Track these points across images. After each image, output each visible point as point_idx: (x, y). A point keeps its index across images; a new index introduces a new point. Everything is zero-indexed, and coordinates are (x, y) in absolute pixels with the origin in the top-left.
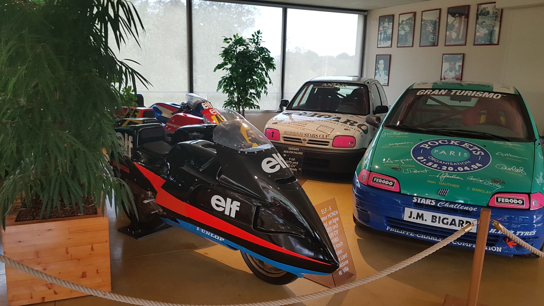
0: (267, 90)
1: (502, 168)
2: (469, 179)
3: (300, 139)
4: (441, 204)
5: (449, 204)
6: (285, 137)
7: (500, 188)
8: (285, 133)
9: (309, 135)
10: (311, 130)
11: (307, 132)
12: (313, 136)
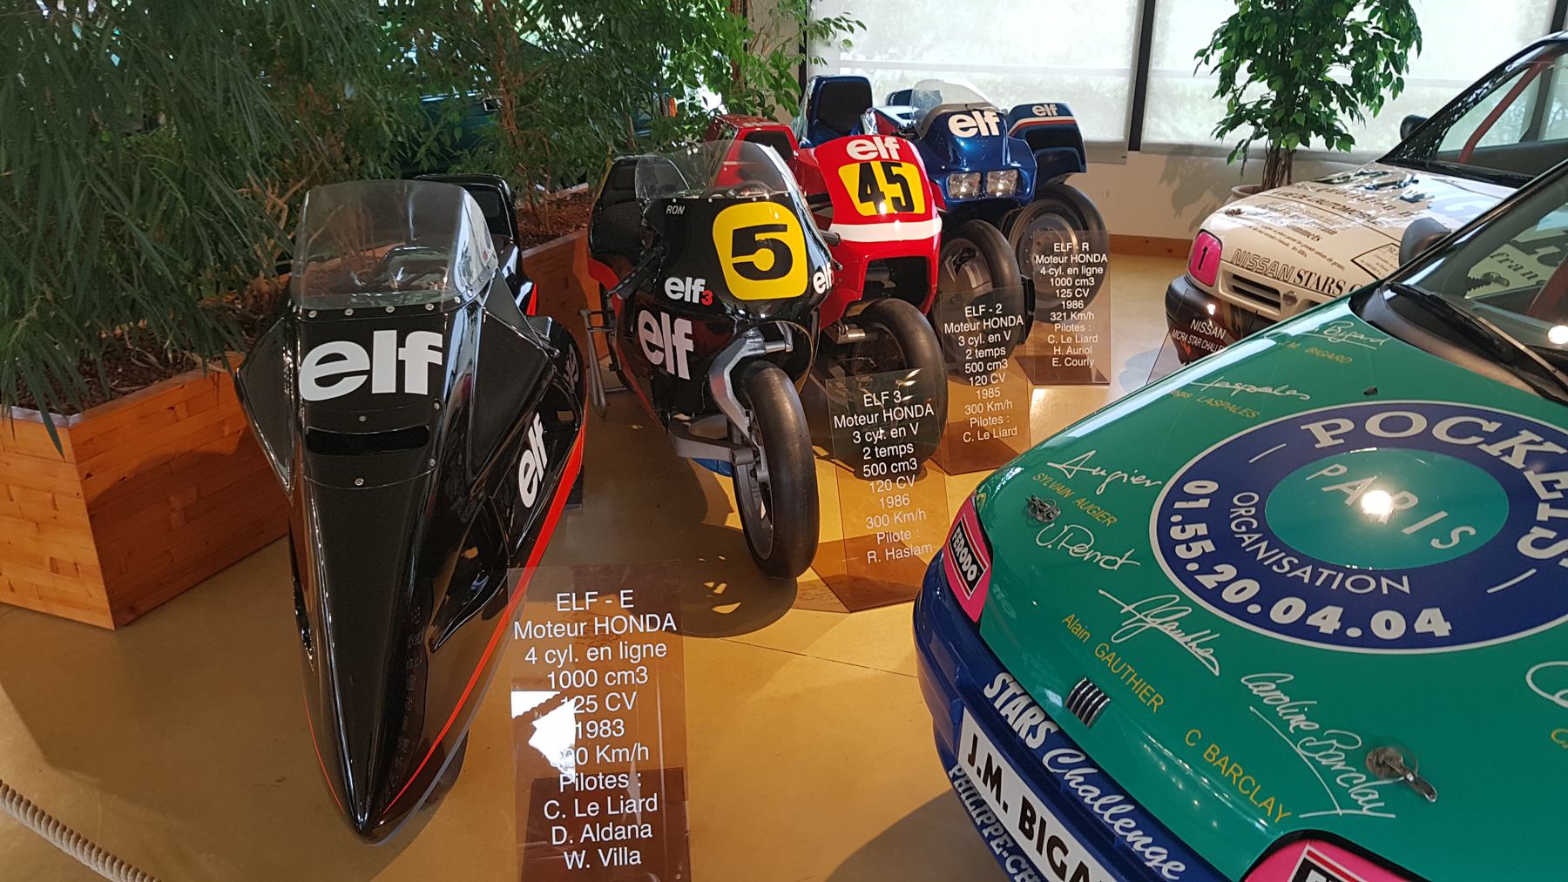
0: (1404, 71)
1: (1556, 698)
2: (1250, 686)
3: (1276, 292)
4: (1061, 760)
5: (1088, 780)
6: (1235, 277)
7: (1365, 811)
8: (1238, 258)
9: (1313, 279)
10: (1330, 260)
11: (1312, 264)
12: (1326, 291)
